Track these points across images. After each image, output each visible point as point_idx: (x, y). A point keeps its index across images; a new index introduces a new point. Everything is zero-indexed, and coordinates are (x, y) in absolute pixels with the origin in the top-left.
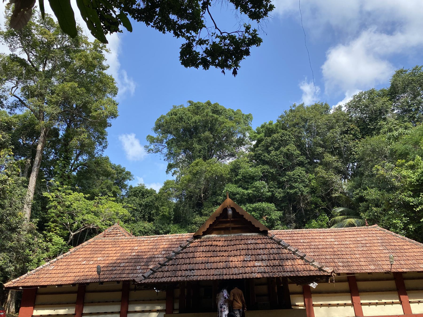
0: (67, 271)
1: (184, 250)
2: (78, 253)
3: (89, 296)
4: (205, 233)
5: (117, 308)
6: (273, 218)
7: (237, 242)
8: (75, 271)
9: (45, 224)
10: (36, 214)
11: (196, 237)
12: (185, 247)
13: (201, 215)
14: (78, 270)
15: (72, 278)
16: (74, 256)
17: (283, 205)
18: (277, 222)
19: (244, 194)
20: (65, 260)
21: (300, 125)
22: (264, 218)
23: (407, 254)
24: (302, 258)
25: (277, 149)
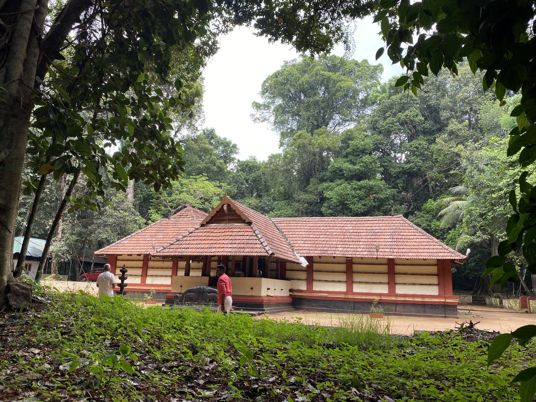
0: (136, 245)
1: (190, 235)
2: (146, 231)
3: (151, 264)
4: (208, 223)
6: (382, 197)
7: (227, 230)
8: (141, 245)
10: (142, 191)
11: (202, 225)
12: (191, 233)
13: (306, 192)
14: (143, 245)
15: (139, 250)
18: (388, 201)
19: (350, 170)
20: (136, 237)
23: (407, 244)
24: (261, 243)
25: (395, 115)
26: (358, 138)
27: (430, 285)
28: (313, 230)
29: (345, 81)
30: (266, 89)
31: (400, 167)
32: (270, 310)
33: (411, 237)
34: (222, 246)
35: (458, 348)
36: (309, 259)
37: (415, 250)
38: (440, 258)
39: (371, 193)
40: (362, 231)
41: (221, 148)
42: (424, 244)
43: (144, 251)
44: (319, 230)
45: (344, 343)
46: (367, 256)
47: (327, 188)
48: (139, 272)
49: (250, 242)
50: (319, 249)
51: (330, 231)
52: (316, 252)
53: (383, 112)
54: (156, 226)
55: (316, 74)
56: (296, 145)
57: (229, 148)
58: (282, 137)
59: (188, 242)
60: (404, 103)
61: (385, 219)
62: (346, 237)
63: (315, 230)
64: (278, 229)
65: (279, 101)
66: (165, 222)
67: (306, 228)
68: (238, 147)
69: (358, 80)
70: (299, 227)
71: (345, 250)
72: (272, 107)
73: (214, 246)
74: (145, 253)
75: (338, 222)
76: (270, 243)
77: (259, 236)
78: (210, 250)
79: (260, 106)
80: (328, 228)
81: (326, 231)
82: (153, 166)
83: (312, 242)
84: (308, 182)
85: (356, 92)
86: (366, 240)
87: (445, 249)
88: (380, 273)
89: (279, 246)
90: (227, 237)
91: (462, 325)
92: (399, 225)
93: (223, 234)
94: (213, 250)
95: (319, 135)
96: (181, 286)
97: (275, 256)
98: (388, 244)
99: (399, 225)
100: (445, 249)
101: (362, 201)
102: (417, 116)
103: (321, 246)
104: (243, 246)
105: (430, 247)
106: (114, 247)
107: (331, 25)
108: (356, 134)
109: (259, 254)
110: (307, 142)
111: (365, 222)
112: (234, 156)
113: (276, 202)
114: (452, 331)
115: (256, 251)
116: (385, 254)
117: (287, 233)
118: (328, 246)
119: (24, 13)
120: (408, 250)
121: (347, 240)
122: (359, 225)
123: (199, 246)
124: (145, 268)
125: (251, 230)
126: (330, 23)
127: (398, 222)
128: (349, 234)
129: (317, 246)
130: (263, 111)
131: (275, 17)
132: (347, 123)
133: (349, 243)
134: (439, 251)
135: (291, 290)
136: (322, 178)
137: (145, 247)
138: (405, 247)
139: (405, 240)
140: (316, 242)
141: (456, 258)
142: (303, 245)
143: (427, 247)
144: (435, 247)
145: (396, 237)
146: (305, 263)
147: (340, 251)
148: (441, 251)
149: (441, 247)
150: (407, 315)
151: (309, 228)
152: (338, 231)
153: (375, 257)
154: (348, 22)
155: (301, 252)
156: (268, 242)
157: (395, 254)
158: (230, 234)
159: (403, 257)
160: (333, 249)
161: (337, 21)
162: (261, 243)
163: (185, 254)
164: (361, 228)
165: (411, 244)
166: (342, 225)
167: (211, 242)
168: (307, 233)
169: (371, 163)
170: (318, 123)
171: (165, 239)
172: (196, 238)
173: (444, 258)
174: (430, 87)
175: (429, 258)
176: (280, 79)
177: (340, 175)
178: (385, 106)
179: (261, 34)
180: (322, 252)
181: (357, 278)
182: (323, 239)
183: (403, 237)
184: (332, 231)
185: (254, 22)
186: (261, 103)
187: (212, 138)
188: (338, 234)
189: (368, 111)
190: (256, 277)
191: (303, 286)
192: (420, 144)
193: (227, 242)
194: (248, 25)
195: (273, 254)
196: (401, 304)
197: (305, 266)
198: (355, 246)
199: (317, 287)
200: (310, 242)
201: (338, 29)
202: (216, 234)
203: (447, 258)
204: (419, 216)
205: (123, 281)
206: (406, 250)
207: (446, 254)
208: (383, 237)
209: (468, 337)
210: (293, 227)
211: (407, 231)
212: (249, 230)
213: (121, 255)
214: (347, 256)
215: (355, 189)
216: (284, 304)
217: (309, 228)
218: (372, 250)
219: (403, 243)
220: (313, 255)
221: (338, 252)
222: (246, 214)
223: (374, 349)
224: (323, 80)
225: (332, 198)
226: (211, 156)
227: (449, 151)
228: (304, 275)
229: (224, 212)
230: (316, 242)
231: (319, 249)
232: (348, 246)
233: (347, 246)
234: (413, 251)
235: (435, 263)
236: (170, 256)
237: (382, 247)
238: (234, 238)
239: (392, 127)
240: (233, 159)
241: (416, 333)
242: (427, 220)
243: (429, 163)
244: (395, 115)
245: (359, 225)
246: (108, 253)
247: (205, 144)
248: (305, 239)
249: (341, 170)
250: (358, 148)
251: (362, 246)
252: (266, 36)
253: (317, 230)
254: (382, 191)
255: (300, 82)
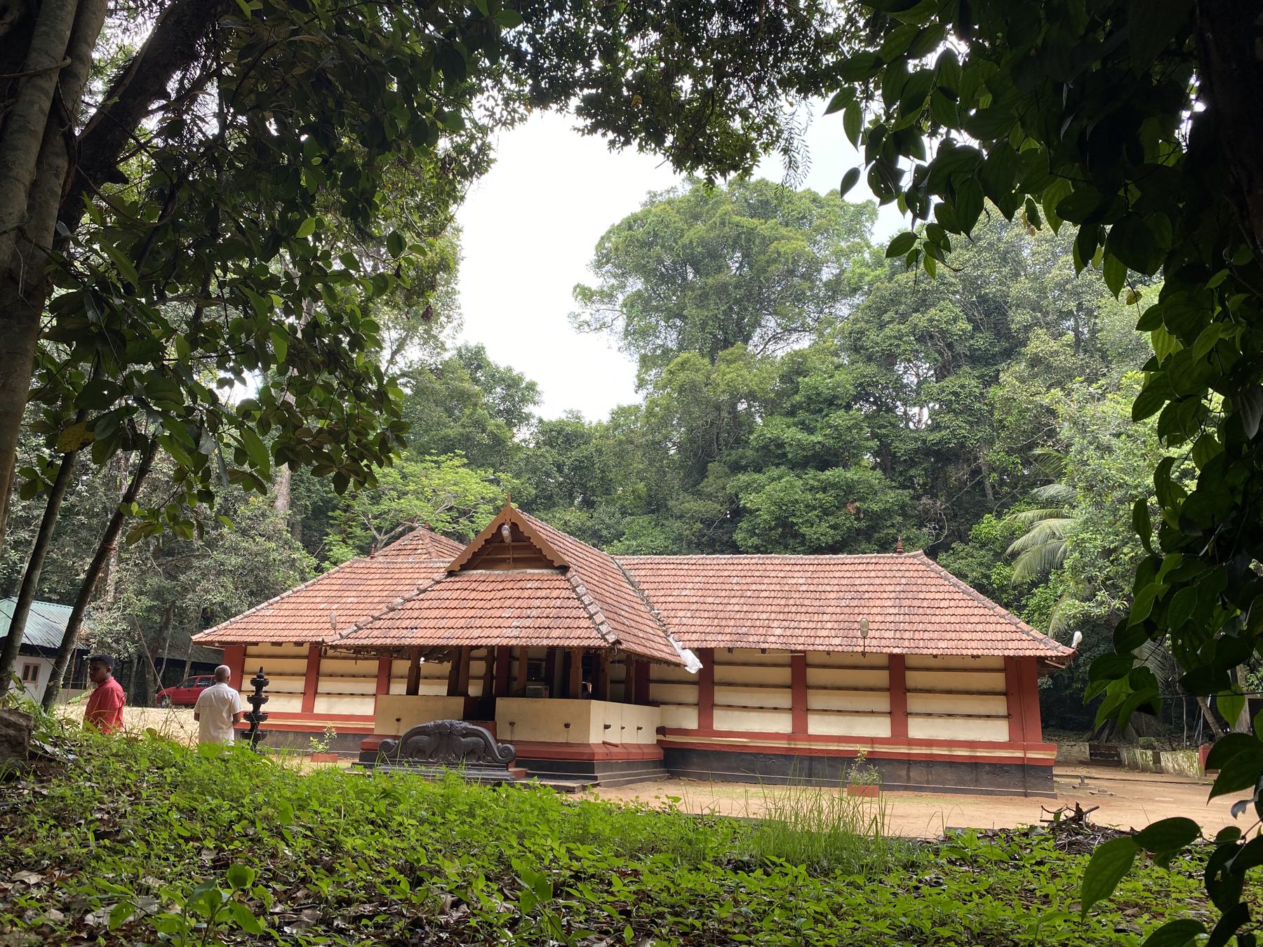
0: (292, 619)
1: (421, 596)
2: (318, 587)
3: (326, 665)
4: (465, 567)
5: (371, 687)
6: (875, 507)
7: (510, 585)
9: (330, 514)
10: (309, 490)
11: (451, 573)
12: (425, 591)
13: (699, 494)
14: (310, 619)
16: (310, 594)
17: (912, 472)
18: (891, 517)
19: (800, 445)
20: (293, 600)
21: (981, 243)
22: (851, 508)
23: (933, 619)
24: (591, 617)
25: (903, 318)
26: (820, 370)
27: (988, 716)
28: (714, 587)
29: (789, 239)
30: (606, 255)
31: (916, 440)
32: (610, 777)
33: (943, 604)
34: (497, 622)
35: (1045, 869)
36: (704, 654)
37: (953, 635)
38: (1011, 653)
39: (851, 498)
40: (828, 588)
41: (498, 390)
42: (973, 619)
43: (311, 635)
44: (727, 587)
45: (774, 859)
46: (840, 648)
47: (747, 487)
48: (299, 685)
49: (565, 613)
50: (728, 630)
51: (754, 587)
52: (720, 637)
53: (878, 311)
54: (341, 575)
55: (723, 224)
56: (676, 384)
57: (518, 391)
58: (642, 367)
59: (416, 614)
60: (925, 290)
61: (882, 561)
62: (791, 602)
63: (719, 586)
64: (632, 584)
65: (636, 284)
66: (362, 565)
67: (697, 579)
68: (538, 388)
69: (818, 238)
70: (680, 579)
71: (788, 632)
72: (621, 298)
73: (478, 622)
74: (314, 639)
75: (772, 567)
76: (611, 615)
77: (586, 600)
78: (468, 633)
79: (592, 294)
80: (749, 580)
81: (745, 587)
82: (334, 435)
83: (711, 614)
84: (703, 473)
85: (815, 265)
86: (838, 610)
87: (1023, 632)
88: (871, 689)
89: (633, 624)
90: (508, 603)
91: (1057, 815)
92: (916, 574)
93: (501, 594)
94: (476, 633)
95: (729, 362)
96: (398, 720)
97: (623, 646)
98: (889, 619)
99: (916, 574)
100: (1023, 632)
101: (830, 518)
102: (955, 320)
103: (732, 623)
104: (546, 622)
105: (988, 627)
106: (239, 626)
107: (753, 111)
108: (814, 362)
109: (586, 643)
110: (699, 377)
111: (836, 568)
112: (528, 409)
113: (628, 519)
114: (1033, 828)
115: (579, 636)
116: (883, 642)
117: (652, 593)
118: (749, 623)
119: (32, 76)
120: (936, 635)
121: (794, 609)
122: (822, 575)
123: (443, 623)
124: (313, 675)
125: (567, 585)
126: (751, 106)
127: (911, 567)
128: (797, 595)
129: (724, 623)
130: (598, 306)
131: (625, 92)
132: (795, 336)
133: (798, 617)
134: (1009, 636)
135: (661, 730)
136: (736, 462)
137: (314, 626)
138: (930, 627)
139: (928, 611)
140: (721, 615)
141: (1049, 653)
142: (690, 621)
143: (980, 627)
144: (999, 627)
145: (907, 603)
146: (693, 665)
147: (776, 638)
148: (1014, 636)
149: (1013, 628)
150: (935, 790)
151: (704, 580)
152: (772, 587)
153: (860, 649)
154: (791, 105)
155: (686, 637)
156: (607, 614)
157: (906, 643)
158: (517, 593)
159: (925, 651)
160: (761, 631)
161: (768, 102)
162: (591, 617)
163: (407, 642)
164: (826, 581)
165: (944, 619)
166: (782, 574)
167: (472, 613)
168: (700, 593)
169: (849, 429)
170: (728, 335)
171: (362, 606)
172: (435, 604)
173: (1021, 653)
174: (986, 255)
175: (986, 652)
176: (639, 232)
177: (777, 457)
178: (882, 297)
179: (592, 130)
180: (736, 637)
181: (816, 700)
182: (737, 608)
183: (925, 604)
184: (759, 587)
185: (575, 102)
186: (594, 288)
187: (479, 367)
188: (772, 594)
189: (843, 309)
190: (576, 697)
191: (690, 720)
192: (962, 387)
193: (509, 613)
194: (561, 110)
195: (618, 642)
196: (920, 762)
197: (693, 672)
198: (811, 625)
199: (724, 722)
200: (706, 614)
201: (771, 120)
202: (483, 595)
203: (1028, 653)
204: (963, 554)
205: (257, 707)
206: (931, 635)
207: (1025, 644)
208: (878, 603)
209: (1071, 844)
210: (666, 579)
211: (933, 589)
212: (562, 584)
213: (256, 644)
214: (793, 647)
215: (812, 489)
216: (645, 764)
217: (704, 580)
218: (851, 633)
219: (924, 619)
220: (713, 645)
221: (772, 639)
222: (555, 547)
223: (847, 872)
224: (739, 236)
225: (759, 510)
226: (475, 409)
227: (1031, 402)
228: (691, 694)
229: (503, 541)
230: (721, 615)
231: (728, 630)
232: (796, 624)
233: (792, 624)
234: (949, 635)
235: (1001, 664)
236: (372, 647)
237: (875, 626)
238: (525, 603)
239: (898, 346)
240: (528, 417)
241: (949, 834)
242: (981, 564)
243: (984, 431)
244: (903, 318)
245: (822, 575)
246: (224, 639)
247: (462, 380)
248: (694, 607)
249: (781, 445)
250: (818, 394)
251: (829, 625)
252: (604, 135)
253: (724, 587)
254: (875, 494)
255: (685, 240)
